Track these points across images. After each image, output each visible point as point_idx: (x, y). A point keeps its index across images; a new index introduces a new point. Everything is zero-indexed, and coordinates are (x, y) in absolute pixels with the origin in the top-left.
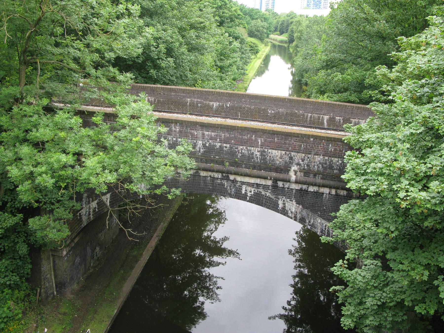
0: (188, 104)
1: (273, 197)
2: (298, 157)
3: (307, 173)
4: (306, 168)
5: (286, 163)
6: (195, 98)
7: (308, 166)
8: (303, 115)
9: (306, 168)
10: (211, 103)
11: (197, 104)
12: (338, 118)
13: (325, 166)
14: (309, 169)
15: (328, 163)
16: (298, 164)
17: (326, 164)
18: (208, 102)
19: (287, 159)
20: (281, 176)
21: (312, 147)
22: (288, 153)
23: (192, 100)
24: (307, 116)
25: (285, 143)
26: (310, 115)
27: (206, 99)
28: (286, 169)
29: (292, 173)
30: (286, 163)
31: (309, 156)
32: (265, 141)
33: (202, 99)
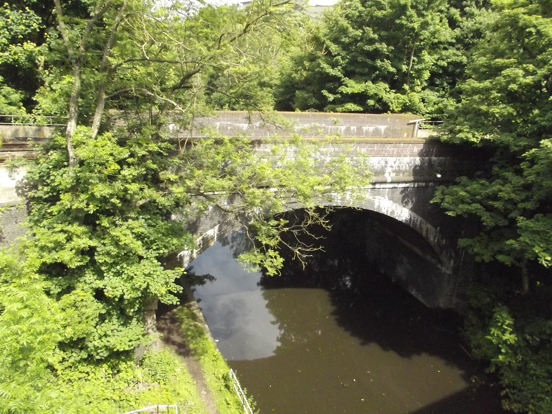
0: (217, 128)
1: (371, 198)
2: (391, 160)
3: (397, 172)
4: (397, 168)
5: (382, 167)
6: (224, 121)
7: (398, 167)
8: (325, 128)
9: (397, 168)
10: (241, 125)
11: (227, 127)
12: (352, 128)
13: (410, 165)
14: (399, 170)
15: (413, 162)
16: (392, 167)
17: (411, 163)
18: (238, 124)
19: (383, 163)
20: (379, 179)
21: (402, 151)
22: (384, 158)
23: (221, 124)
24: (328, 128)
25: (382, 150)
26: (330, 127)
27: (236, 121)
28: (381, 172)
29: (386, 175)
30: (382, 167)
31: (400, 158)
32: (367, 150)
33: (232, 121)
